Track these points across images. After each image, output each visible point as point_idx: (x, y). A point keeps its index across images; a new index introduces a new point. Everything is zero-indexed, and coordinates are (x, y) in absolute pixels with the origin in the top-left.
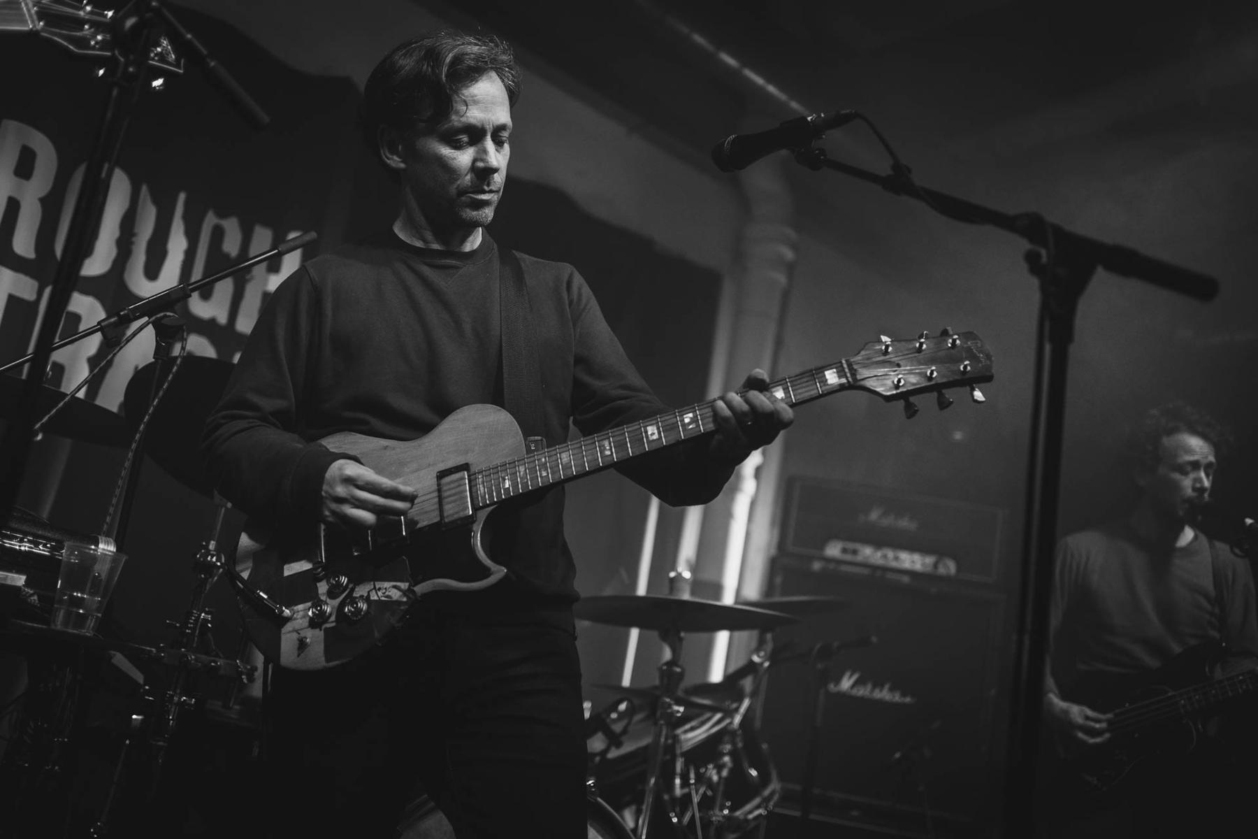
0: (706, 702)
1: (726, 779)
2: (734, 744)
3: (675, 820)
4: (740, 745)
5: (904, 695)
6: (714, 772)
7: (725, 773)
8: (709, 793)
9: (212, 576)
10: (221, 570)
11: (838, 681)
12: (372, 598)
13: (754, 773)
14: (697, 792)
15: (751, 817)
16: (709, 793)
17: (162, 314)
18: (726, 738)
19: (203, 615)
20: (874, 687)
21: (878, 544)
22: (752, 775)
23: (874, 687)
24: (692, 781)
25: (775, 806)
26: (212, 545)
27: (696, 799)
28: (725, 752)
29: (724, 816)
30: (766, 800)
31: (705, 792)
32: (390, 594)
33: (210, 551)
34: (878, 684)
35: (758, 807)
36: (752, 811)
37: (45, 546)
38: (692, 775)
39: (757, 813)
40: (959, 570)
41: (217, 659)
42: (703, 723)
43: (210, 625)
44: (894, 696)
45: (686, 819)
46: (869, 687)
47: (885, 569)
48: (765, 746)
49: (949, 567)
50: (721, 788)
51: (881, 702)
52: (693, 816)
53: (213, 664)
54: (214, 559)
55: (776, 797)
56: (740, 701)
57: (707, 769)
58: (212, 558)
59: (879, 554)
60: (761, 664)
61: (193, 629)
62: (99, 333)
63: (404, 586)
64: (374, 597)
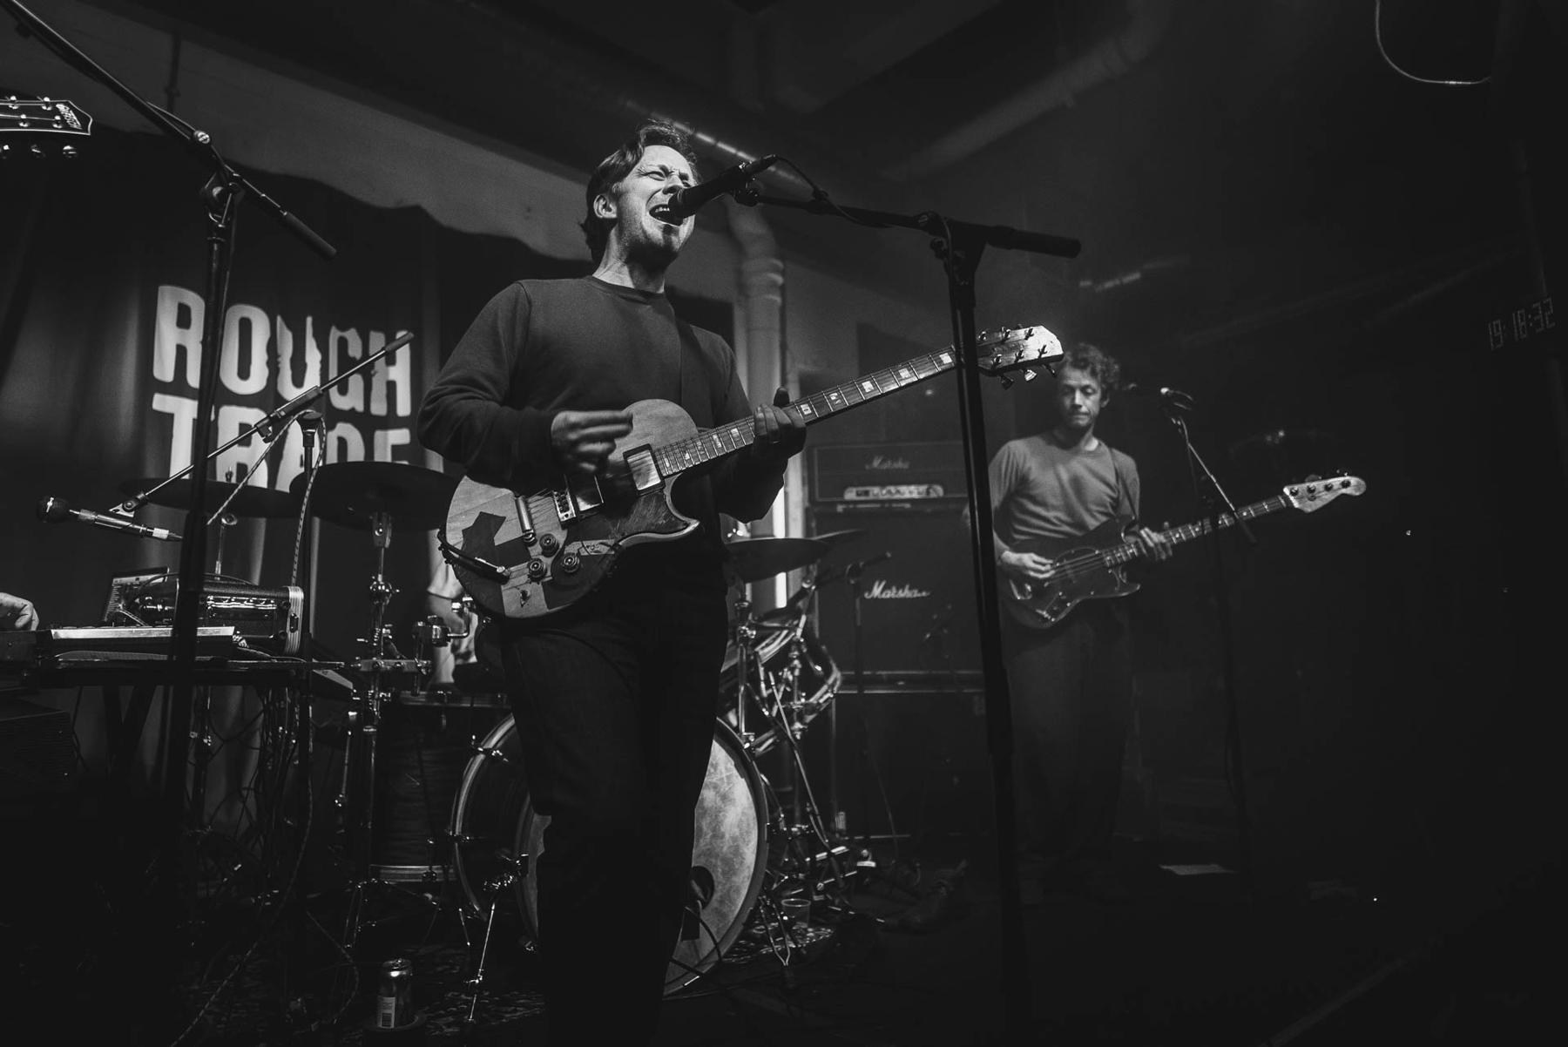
0: (775, 625)
1: (798, 677)
2: (800, 650)
3: (767, 713)
4: (805, 650)
5: (920, 591)
6: (789, 673)
7: (797, 673)
8: (788, 689)
11: (870, 590)
14: (778, 691)
15: (821, 701)
16: (788, 689)
17: (303, 412)
18: (793, 647)
20: (898, 589)
21: (883, 485)
23: (898, 589)
24: (773, 683)
25: (839, 689)
26: (380, 578)
27: (779, 697)
29: (802, 704)
30: (832, 686)
31: (785, 689)
34: (900, 587)
35: (826, 692)
36: (822, 696)
37: (248, 601)
38: (772, 678)
39: (826, 697)
40: (945, 491)
42: (774, 640)
44: (913, 594)
46: (894, 589)
47: (891, 501)
48: (824, 647)
49: (938, 491)
50: (796, 684)
51: (904, 600)
52: (779, 708)
55: (838, 683)
56: (799, 619)
57: (783, 672)
59: (884, 492)
60: (810, 588)
61: (378, 642)
62: (257, 433)
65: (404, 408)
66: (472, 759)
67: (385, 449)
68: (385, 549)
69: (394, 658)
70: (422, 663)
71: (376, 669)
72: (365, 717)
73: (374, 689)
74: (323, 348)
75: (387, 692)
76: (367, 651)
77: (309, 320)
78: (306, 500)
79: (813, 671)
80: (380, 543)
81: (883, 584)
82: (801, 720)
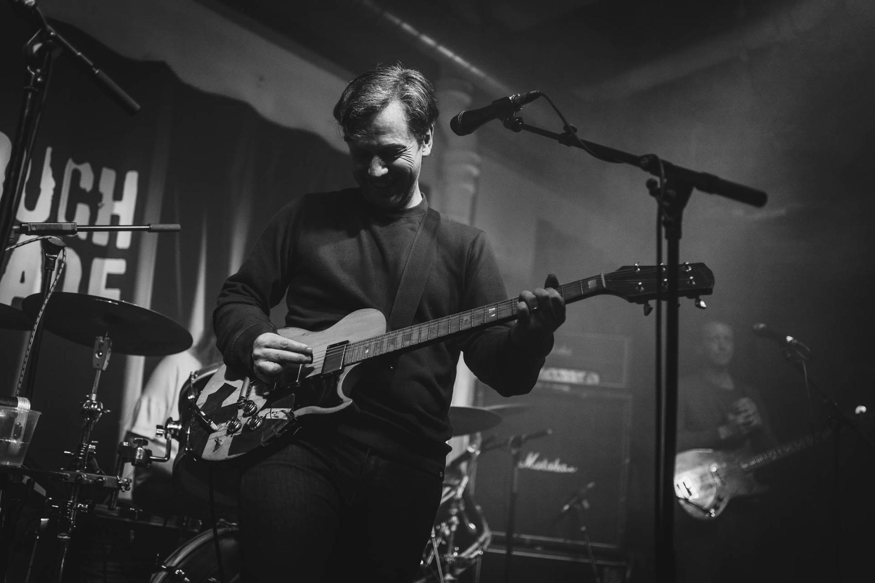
1: (455, 532)
2: (458, 508)
5: (569, 466)
6: (447, 528)
7: (454, 528)
8: (444, 542)
9: (95, 419)
10: (101, 414)
12: (267, 418)
13: (472, 526)
15: (472, 556)
16: (444, 542)
18: (454, 505)
19: (90, 446)
22: (471, 529)
25: (489, 547)
26: (94, 397)
27: (436, 546)
28: (453, 514)
29: (455, 558)
31: (441, 543)
32: (278, 415)
33: (93, 401)
34: (551, 460)
35: (477, 549)
36: (473, 552)
41: (101, 476)
43: (95, 453)
45: (429, 561)
47: (553, 383)
50: (452, 538)
53: (100, 480)
54: (96, 407)
55: (488, 542)
58: (94, 405)
60: (474, 453)
63: (287, 410)
64: (268, 417)
65: (124, 240)
66: (153, 575)
67: (101, 276)
68: (102, 371)
69: (94, 472)
70: (123, 481)
71: (78, 480)
72: (59, 522)
73: (73, 500)
74: (58, 177)
75: (85, 504)
76: (72, 463)
77: (49, 150)
78: (38, 320)
79: (467, 529)
80: (98, 365)
81: (536, 456)
82: (452, 572)
